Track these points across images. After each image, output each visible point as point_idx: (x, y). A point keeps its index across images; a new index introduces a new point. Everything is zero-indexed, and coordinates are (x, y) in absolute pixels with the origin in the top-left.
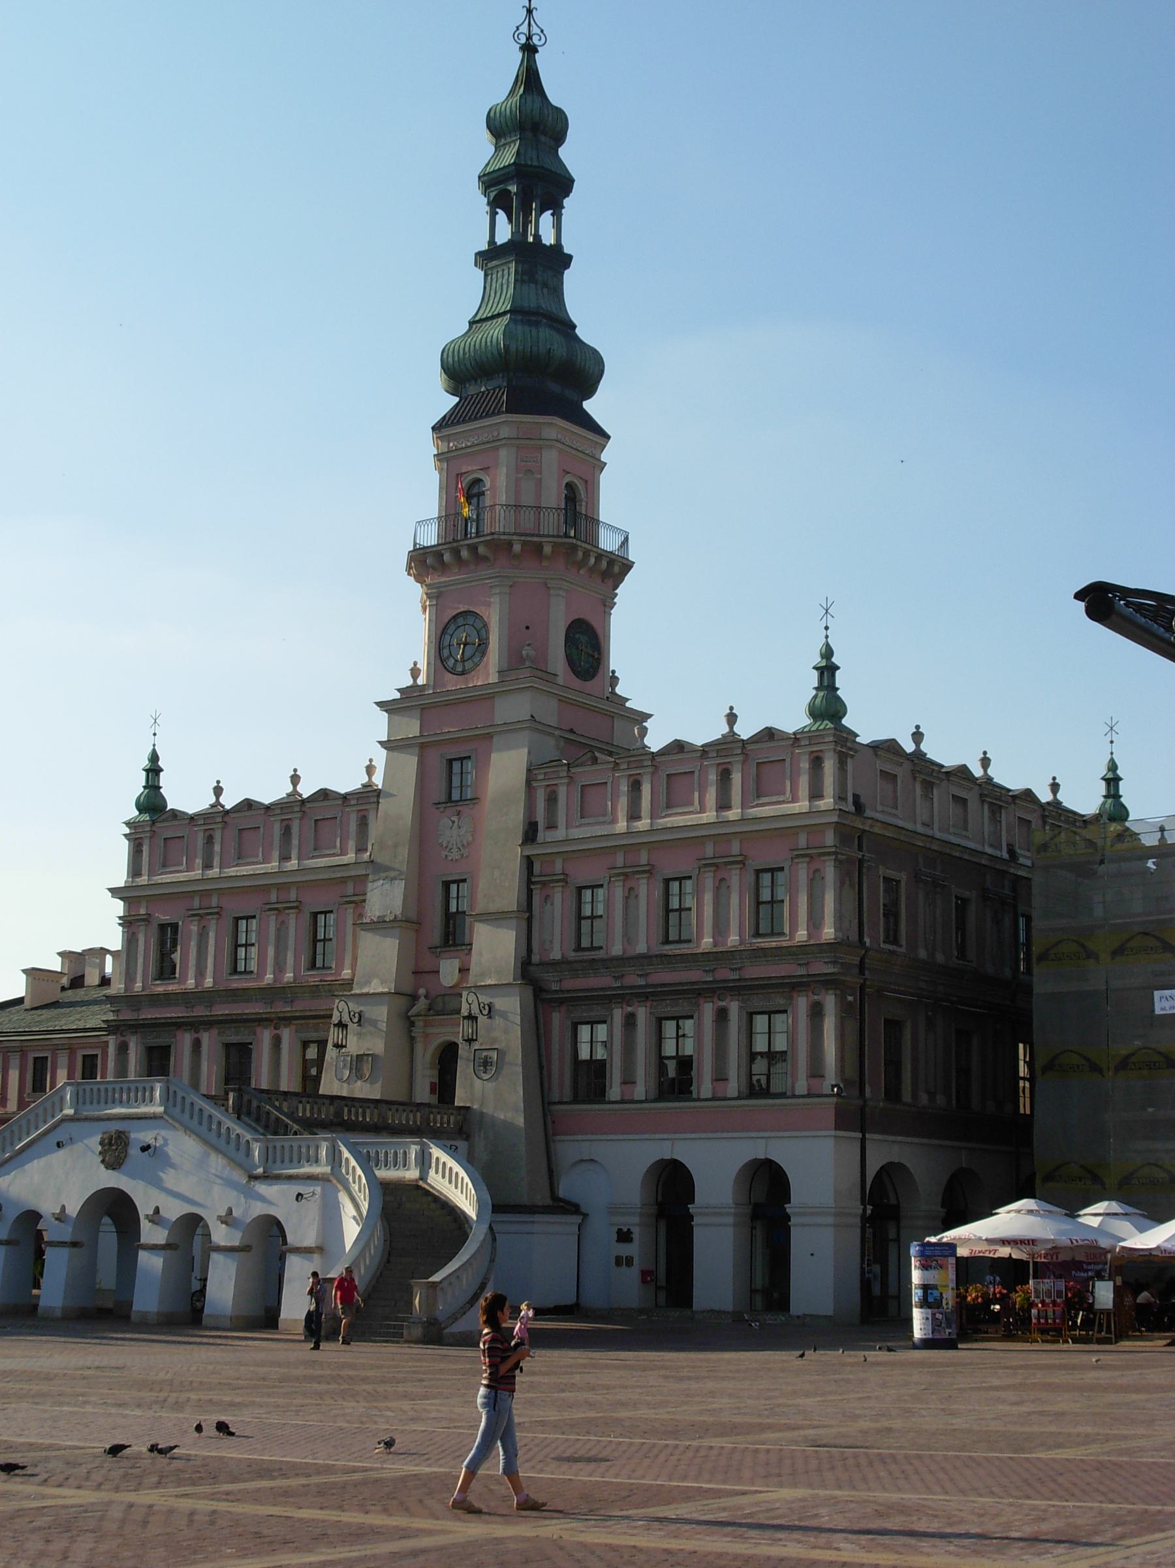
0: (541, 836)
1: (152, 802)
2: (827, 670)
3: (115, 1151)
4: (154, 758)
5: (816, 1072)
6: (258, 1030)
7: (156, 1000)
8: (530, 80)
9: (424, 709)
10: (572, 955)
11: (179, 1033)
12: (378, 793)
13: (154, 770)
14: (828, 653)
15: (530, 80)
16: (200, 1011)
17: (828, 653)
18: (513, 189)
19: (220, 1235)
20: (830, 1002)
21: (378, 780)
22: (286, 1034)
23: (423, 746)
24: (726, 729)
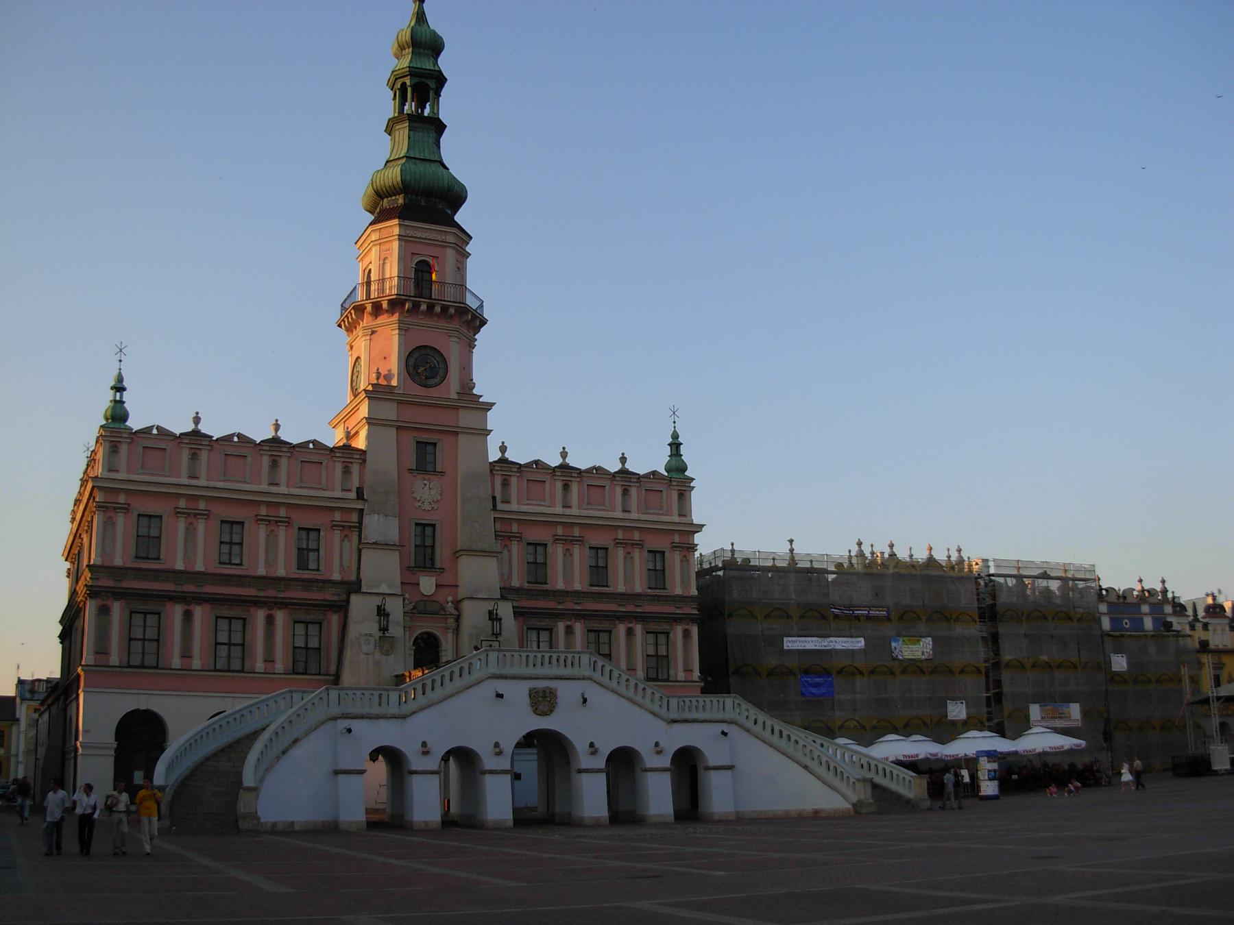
0: (500, 506)
1: (118, 414)
2: (675, 446)
3: (543, 701)
4: (120, 379)
5: (688, 670)
6: (252, 610)
7: (140, 573)
8: (421, 17)
9: (400, 402)
10: (526, 585)
11: (169, 605)
12: (364, 452)
13: (119, 388)
14: (675, 436)
15: (421, 17)
16: (190, 588)
17: (675, 436)
18: (432, 85)
19: (650, 760)
20: (695, 630)
21: (361, 443)
22: (198, 611)
23: (398, 428)
24: (620, 466)
